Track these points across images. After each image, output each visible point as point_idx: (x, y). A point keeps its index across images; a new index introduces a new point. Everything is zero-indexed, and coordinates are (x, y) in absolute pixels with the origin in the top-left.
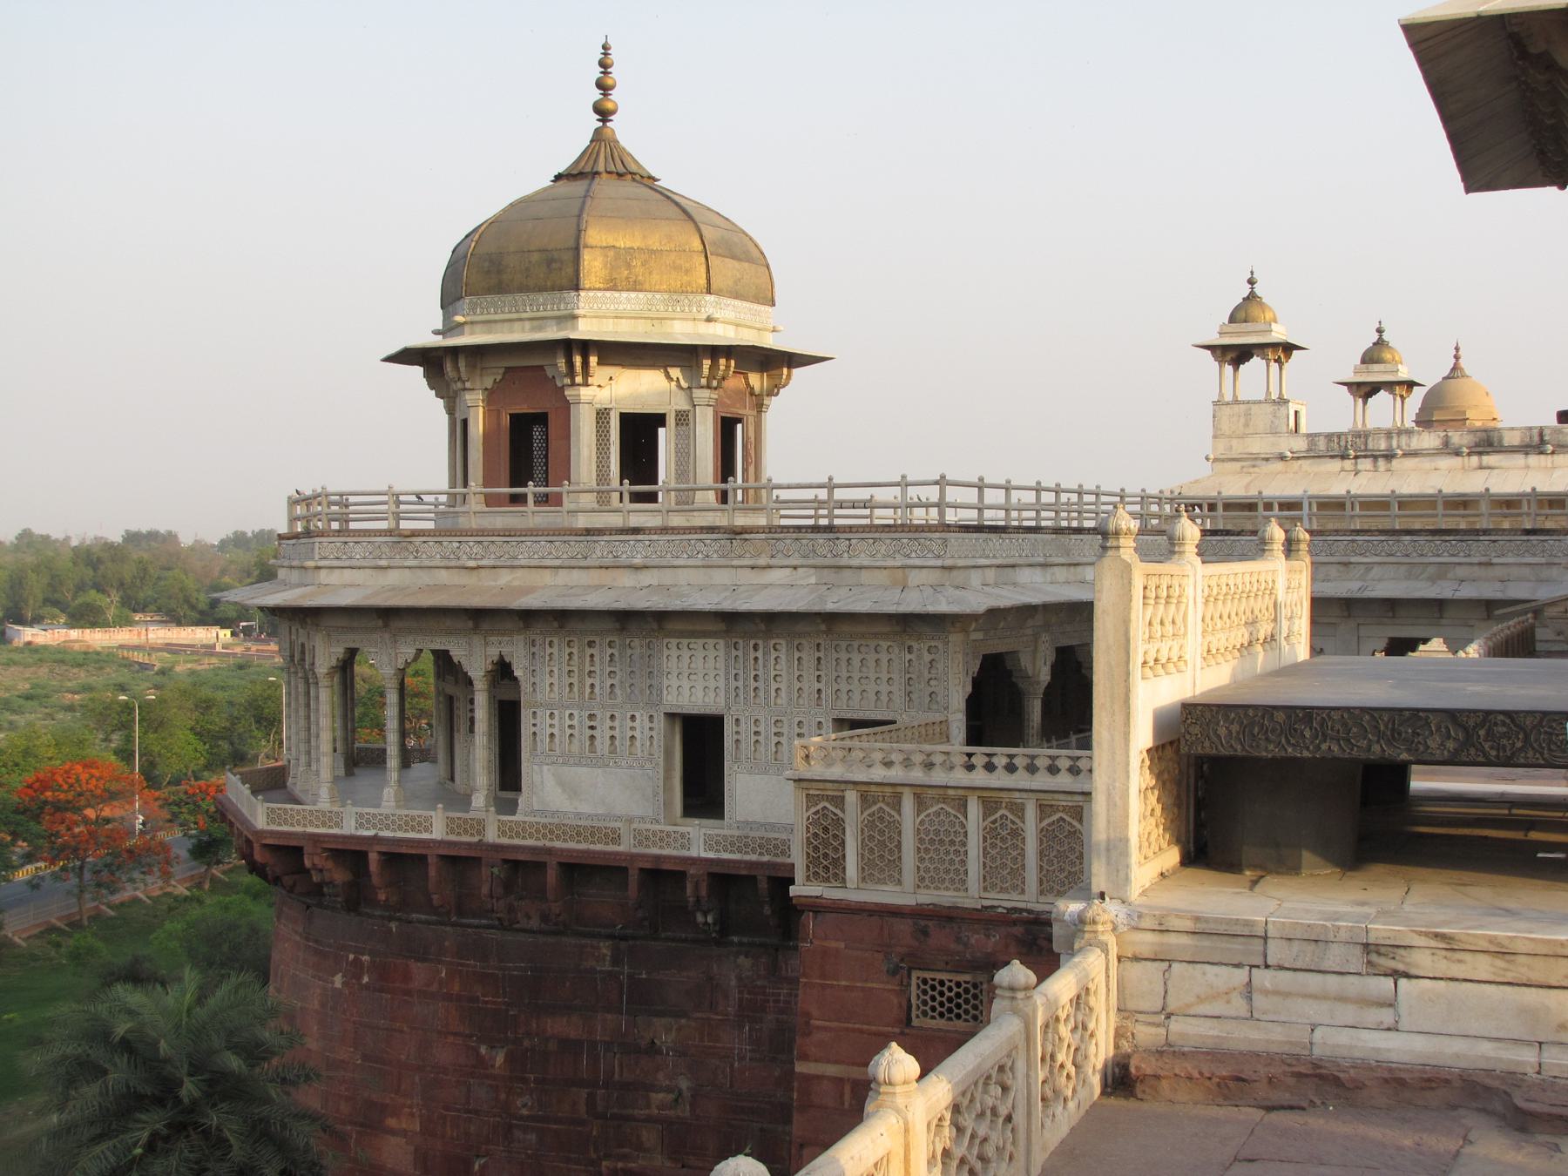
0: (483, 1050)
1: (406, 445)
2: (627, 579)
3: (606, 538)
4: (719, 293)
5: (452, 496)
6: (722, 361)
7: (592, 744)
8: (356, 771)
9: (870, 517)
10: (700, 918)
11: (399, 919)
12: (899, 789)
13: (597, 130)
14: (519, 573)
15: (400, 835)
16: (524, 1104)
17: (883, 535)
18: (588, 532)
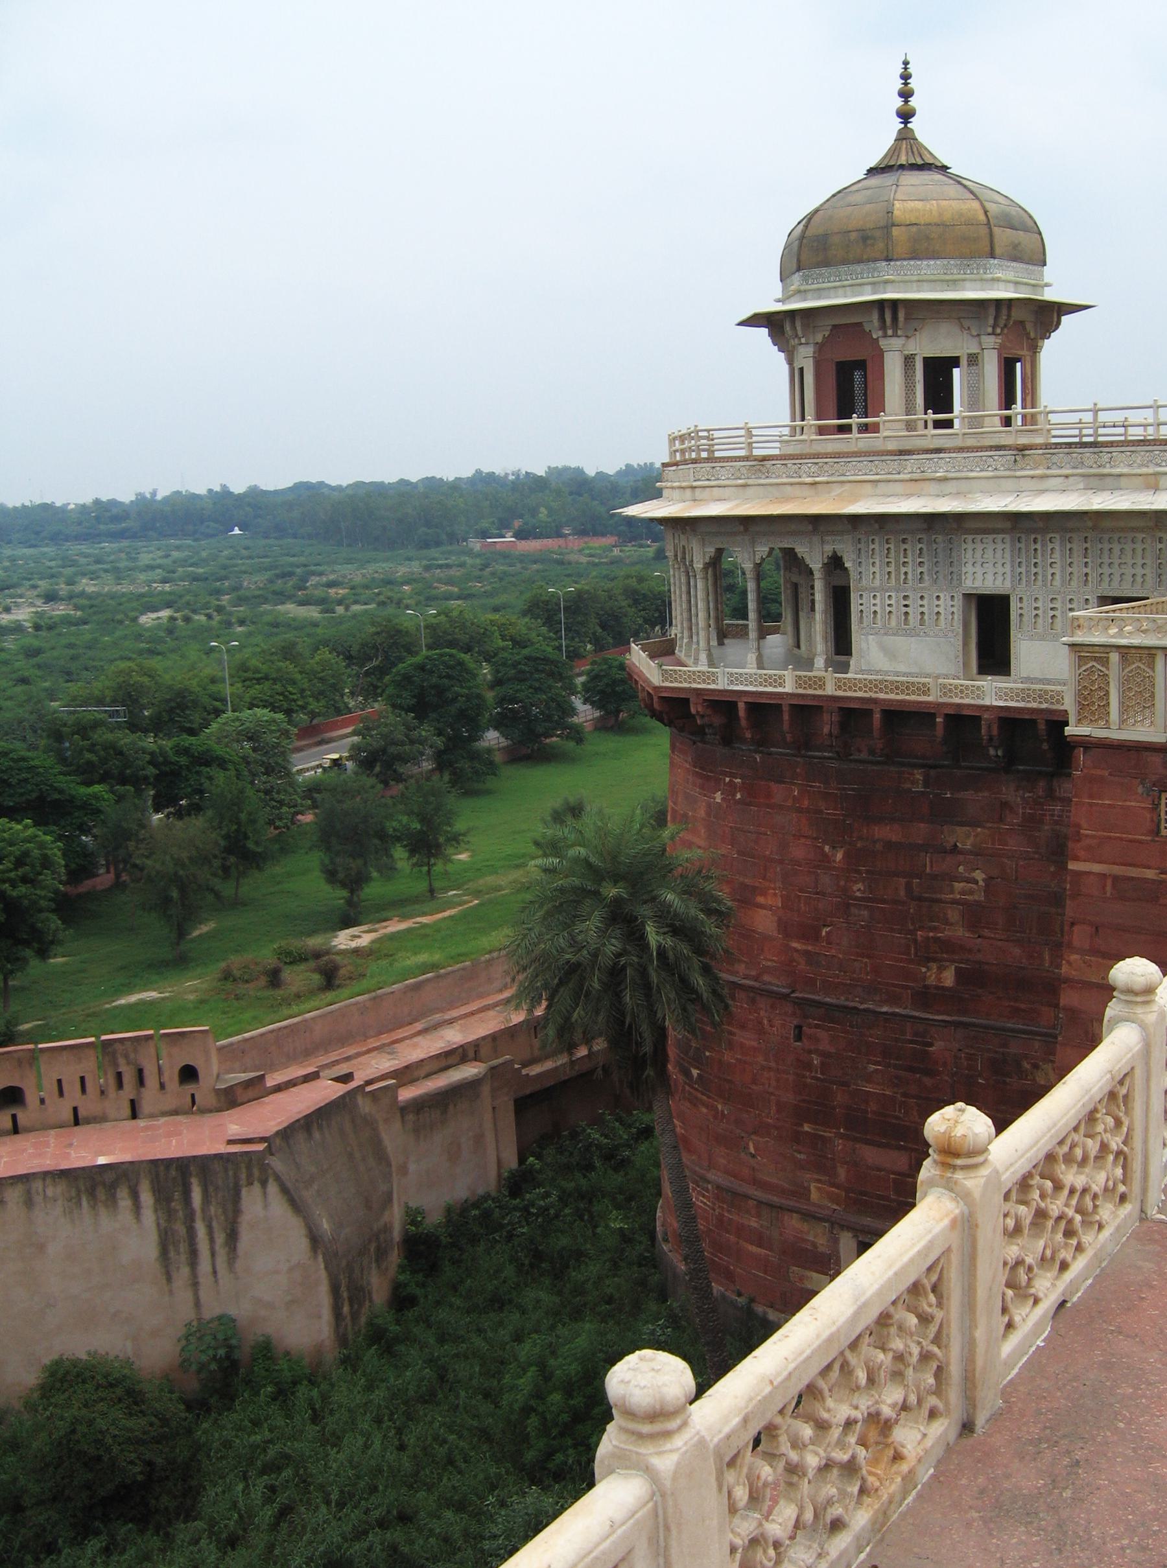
0: (827, 848)
1: (758, 391)
2: (933, 487)
3: (914, 457)
5: (793, 428)
6: (1004, 311)
7: (906, 619)
8: (726, 641)
9: (1125, 434)
10: (992, 752)
11: (761, 752)
12: (1153, 652)
14: (847, 487)
15: (761, 689)
16: (858, 889)
17: (1139, 448)
18: (902, 453)
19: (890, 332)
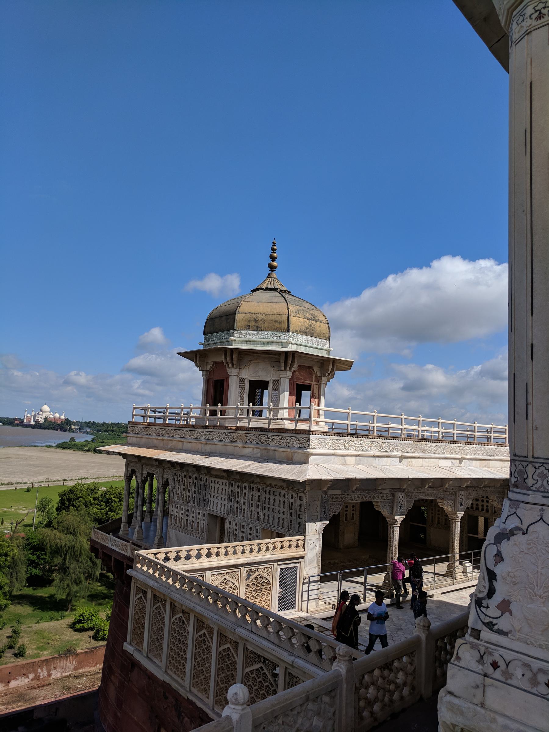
3: (198, 430)
4: (296, 332)
13: (269, 274)
17: (285, 435)
19: (230, 366)
